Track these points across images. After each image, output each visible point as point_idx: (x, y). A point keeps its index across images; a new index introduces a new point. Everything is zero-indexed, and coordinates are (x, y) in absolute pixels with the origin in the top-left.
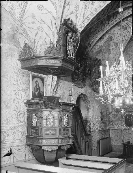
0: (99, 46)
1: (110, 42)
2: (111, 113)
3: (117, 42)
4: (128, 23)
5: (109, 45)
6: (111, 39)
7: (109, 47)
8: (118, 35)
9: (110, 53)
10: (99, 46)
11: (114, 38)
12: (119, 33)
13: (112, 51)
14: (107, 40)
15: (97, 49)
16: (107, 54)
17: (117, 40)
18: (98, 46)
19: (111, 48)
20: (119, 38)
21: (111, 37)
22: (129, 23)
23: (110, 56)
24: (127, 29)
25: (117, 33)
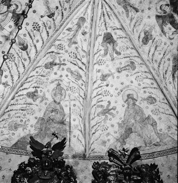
1: (134, 104)
3: (147, 95)
4: (126, 56)
5: (139, 112)
6: (133, 99)
7: (142, 113)
8: (136, 83)
9: (154, 124)
11: (134, 93)
12: (133, 78)
13: (155, 117)
14: (126, 106)
15: (116, 132)
16: (150, 127)
17: (145, 92)
19: (148, 112)
20: (143, 86)
21: (128, 96)
22: (125, 52)
23: (158, 128)
24: (136, 63)
25: (132, 82)
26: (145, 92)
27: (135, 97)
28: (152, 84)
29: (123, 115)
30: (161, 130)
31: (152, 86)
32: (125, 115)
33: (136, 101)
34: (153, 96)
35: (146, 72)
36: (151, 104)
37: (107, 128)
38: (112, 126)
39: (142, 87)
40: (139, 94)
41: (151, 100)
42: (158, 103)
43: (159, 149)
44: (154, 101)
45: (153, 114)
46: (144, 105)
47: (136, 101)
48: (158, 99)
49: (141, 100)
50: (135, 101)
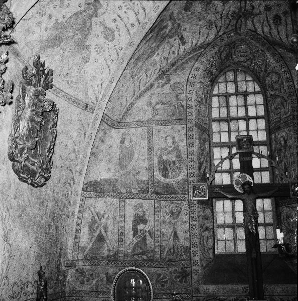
0: (53, 19)
1: (91, 17)
2: (71, 265)
3: (112, 25)
6: (96, 10)
9: (86, 60)
10: (53, 19)
13: (93, 53)
14: (82, 9)
16: (78, 59)
17: (115, 20)
18: (50, 17)
23: (85, 67)
26: (115, 20)
27: (100, 11)
28: (132, 25)
29: (69, 15)
30: (85, 72)
31: (128, 25)
32: (70, 18)
33: (96, 16)
34: (116, 33)
35: (144, 9)
36: (104, 37)
37: (44, 13)
38: (50, 17)
39: (119, 12)
40: (107, 14)
41: (109, 34)
42: (111, 45)
43: (68, 90)
44: (110, 39)
45: (95, 48)
46: (97, 29)
47: (96, 16)
48: (115, 42)
49: (100, 22)
50: (94, 15)
